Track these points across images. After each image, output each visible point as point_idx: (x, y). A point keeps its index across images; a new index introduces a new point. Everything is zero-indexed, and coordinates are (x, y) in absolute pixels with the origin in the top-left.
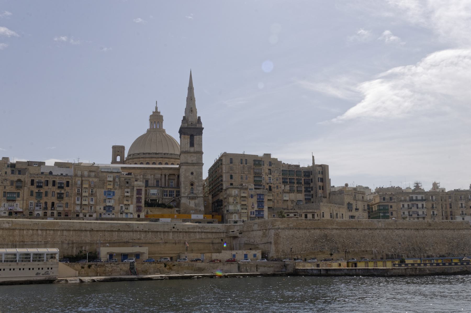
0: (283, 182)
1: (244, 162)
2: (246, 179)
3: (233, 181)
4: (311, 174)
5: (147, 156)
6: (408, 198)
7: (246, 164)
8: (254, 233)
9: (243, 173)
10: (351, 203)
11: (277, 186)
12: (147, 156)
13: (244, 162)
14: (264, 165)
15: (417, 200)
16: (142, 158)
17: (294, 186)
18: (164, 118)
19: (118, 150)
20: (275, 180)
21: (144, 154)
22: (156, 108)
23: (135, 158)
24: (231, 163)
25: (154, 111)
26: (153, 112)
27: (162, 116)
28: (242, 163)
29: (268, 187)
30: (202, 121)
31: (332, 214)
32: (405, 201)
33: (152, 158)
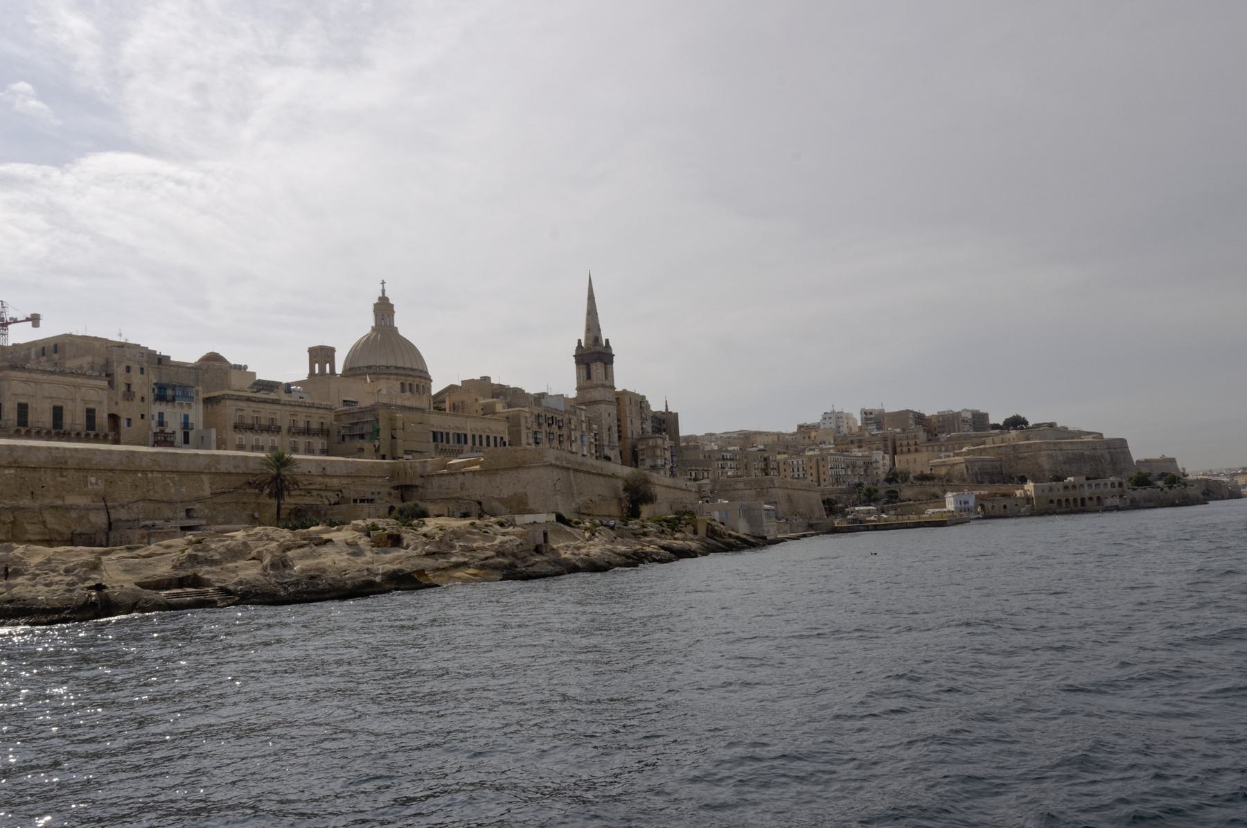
4: (664, 422)
5: (403, 372)
6: (721, 457)
8: (739, 492)
12: (403, 372)
15: (727, 459)
16: (395, 374)
18: (395, 309)
19: (321, 355)
21: (396, 368)
22: (383, 291)
23: (385, 374)
25: (381, 295)
26: (380, 298)
27: (392, 306)
30: (611, 344)
32: (718, 460)
33: (410, 375)
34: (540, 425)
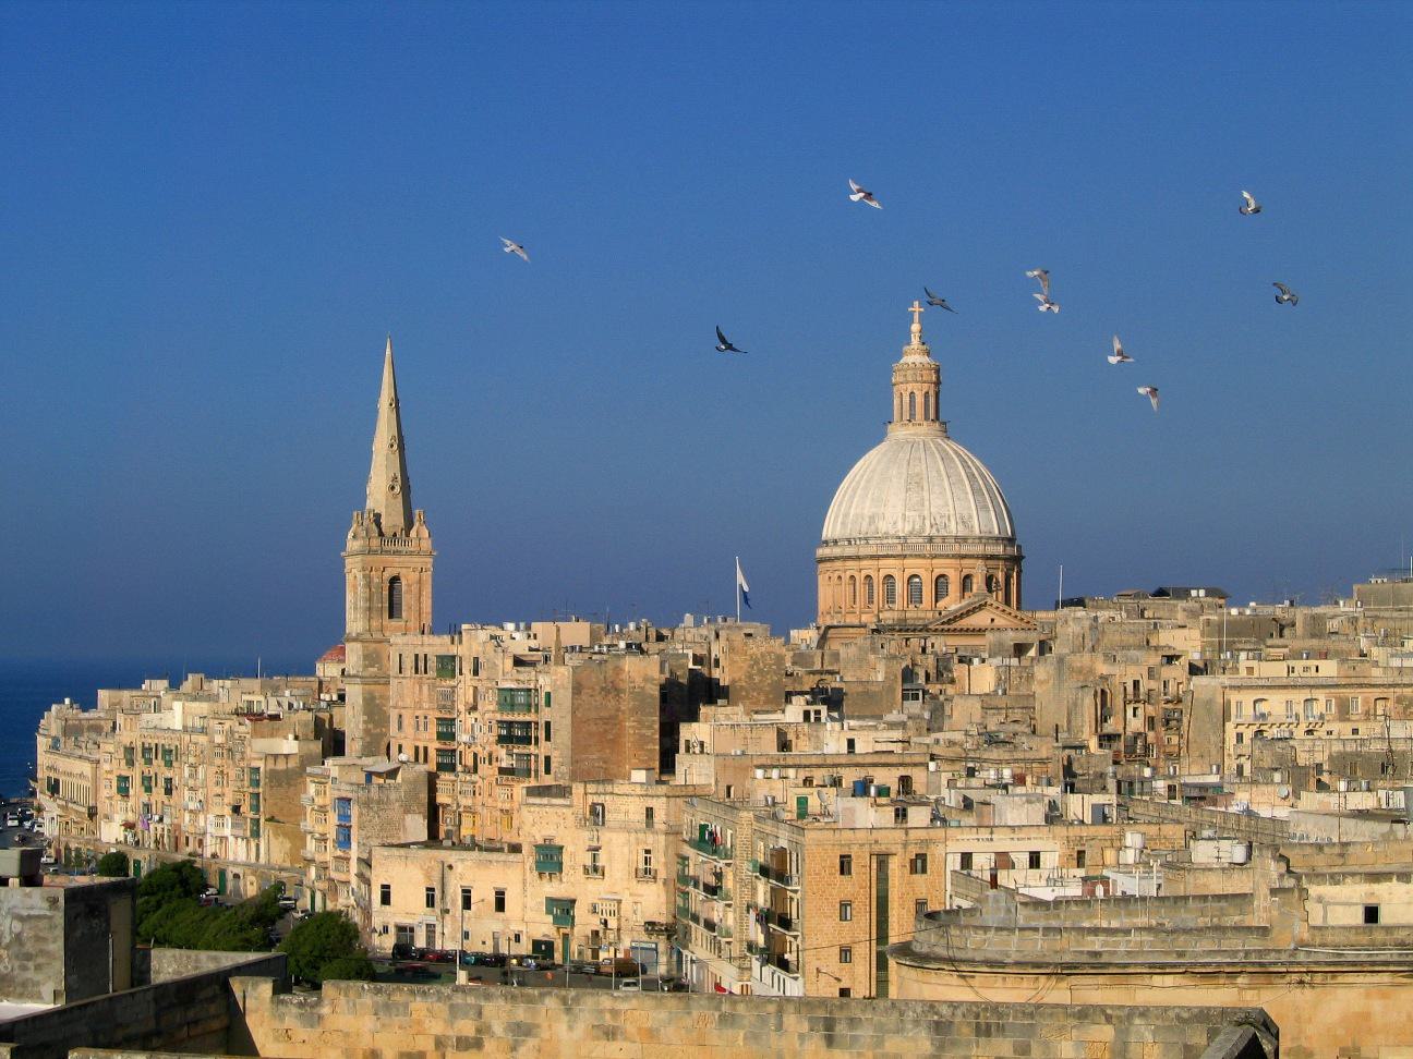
0: (501, 740)
1: (421, 664)
2: (426, 729)
3: (403, 735)
7: (426, 672)
9: (420, 708)
10: (558, 842)
11: (490, 755)
13: (421, 664)
14: (461, 673)
17: (529, 755)
20: (485, 729)
24: (400, 672)
28: (417, 672)
29: (470, 762)
31: (437, 894)
34: (131, 763)
